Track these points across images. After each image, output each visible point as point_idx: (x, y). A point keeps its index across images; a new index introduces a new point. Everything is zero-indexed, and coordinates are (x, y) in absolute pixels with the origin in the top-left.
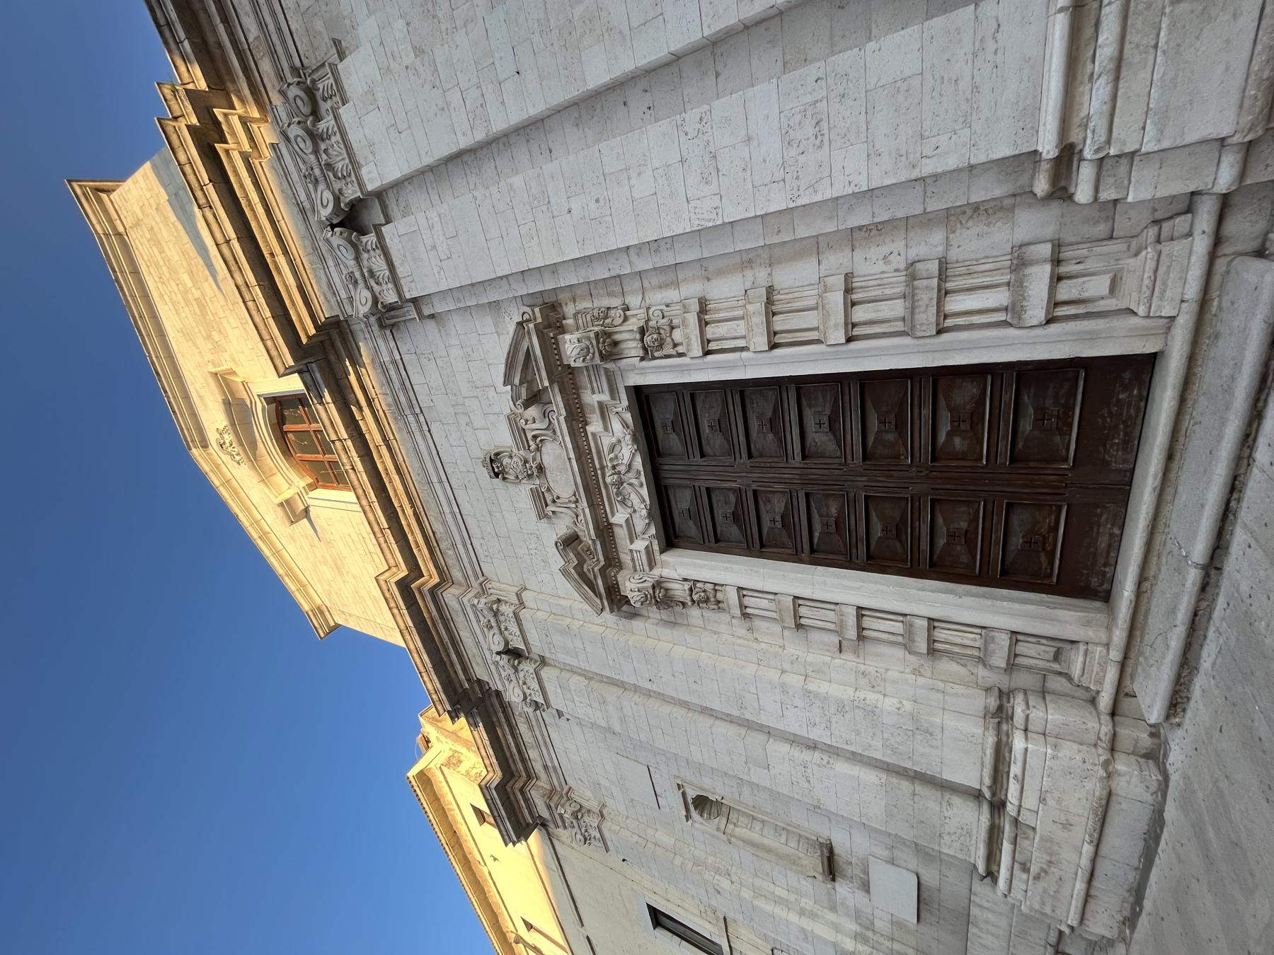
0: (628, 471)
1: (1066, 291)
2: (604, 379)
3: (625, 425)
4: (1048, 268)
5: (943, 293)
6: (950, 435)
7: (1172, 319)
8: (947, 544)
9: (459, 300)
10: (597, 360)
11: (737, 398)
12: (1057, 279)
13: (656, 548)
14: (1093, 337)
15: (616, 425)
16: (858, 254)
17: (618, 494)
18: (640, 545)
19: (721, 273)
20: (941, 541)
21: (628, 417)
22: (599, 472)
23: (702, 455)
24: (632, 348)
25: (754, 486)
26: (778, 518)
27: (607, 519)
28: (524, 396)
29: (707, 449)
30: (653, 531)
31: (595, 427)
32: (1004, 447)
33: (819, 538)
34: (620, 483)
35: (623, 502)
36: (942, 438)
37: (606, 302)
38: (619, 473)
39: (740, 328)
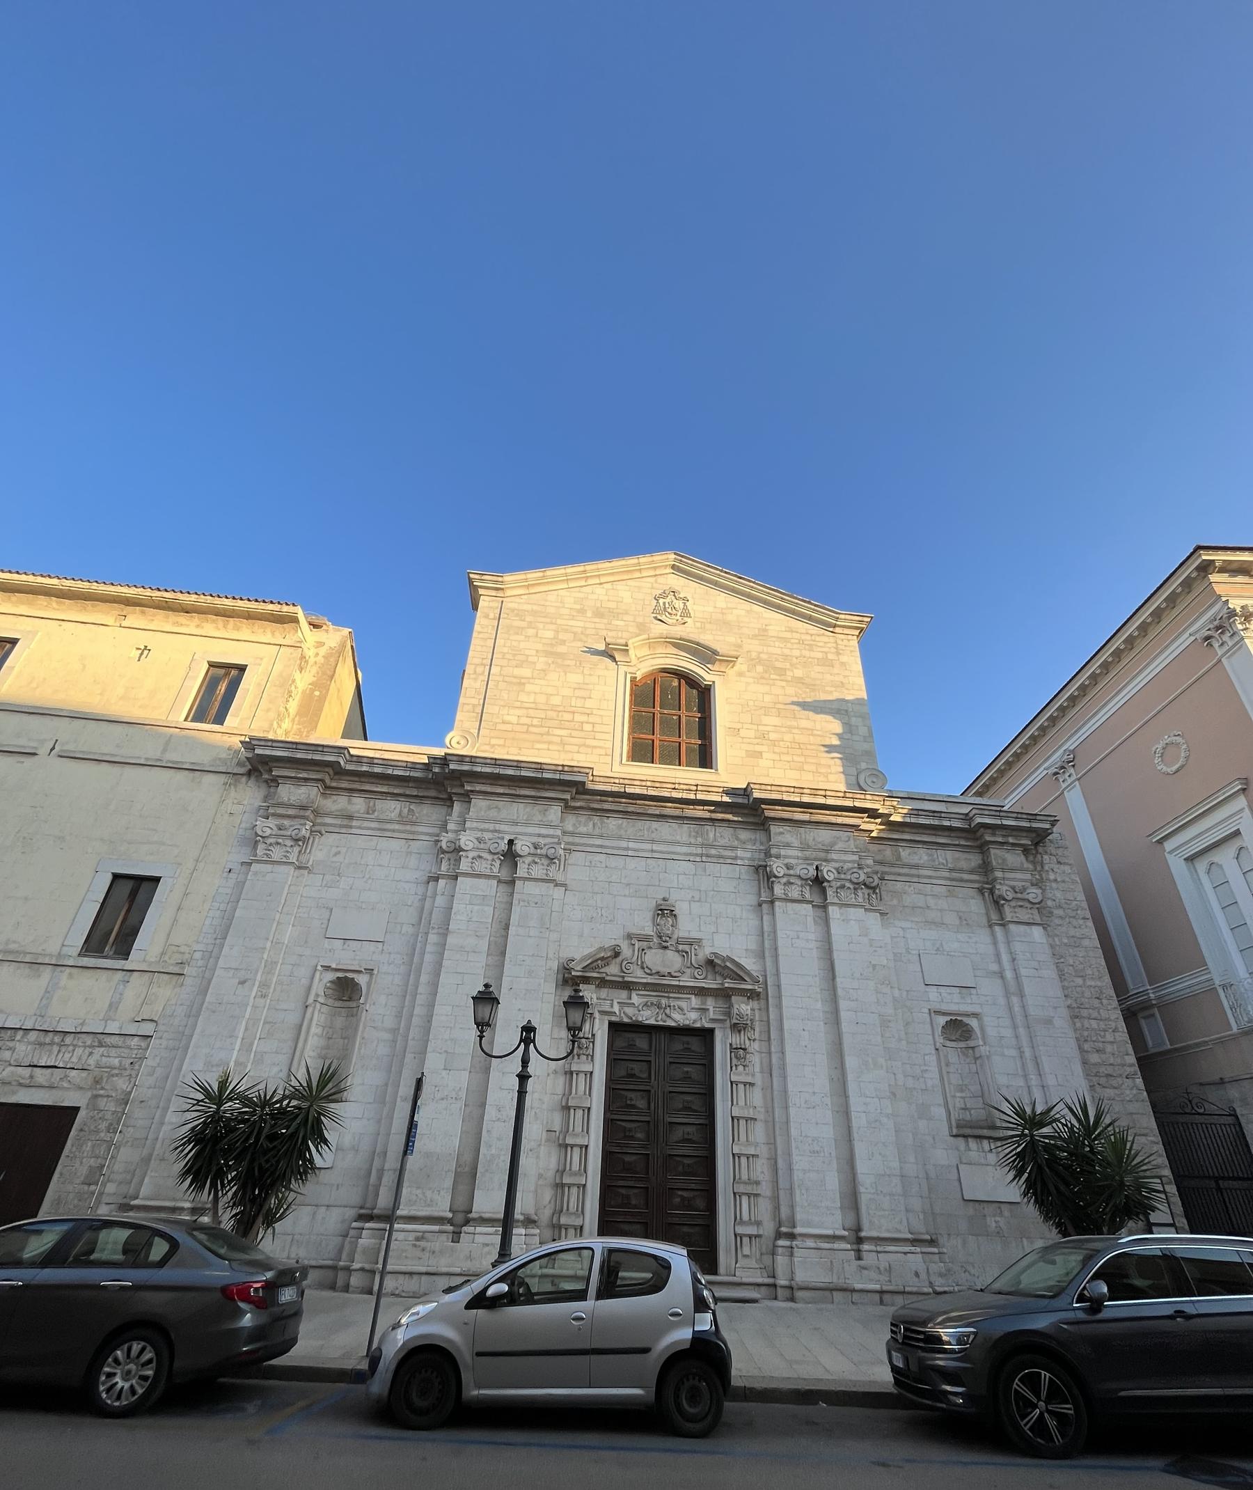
0: (666, 1014)
1: (746, 1240)
2: (721, 1018)
3: (695, 1021)
4: (756, 1233)
5: (749, 1195)
6: (681, 1196)
7: (735, 1276)
8: (623, 1195)
9: (769, 936)
10: (734, 1021)
11: (702, 1091)
12: (750, 1237)
13: (613, 1019)
14: (728, 1251)
15: (693, 1015)
16: (764, 1161)
17: (652, 1004)
18: (616, 1009)
19: (764, 1097)
20: (623, 1191)
21: (698, 1025)
22: (666, 995)
23: (670, 1063)
24: (736, 1040)
25: (653, 1091)
26: (633, 1103)
27: (636, 990)
28: (716, 960)
29: (674, 1066)
30: (626, 1020)
31: (695, 1001)
32: (676, 1220)
33: (621, 1125)
34: (659, 1006)
35: (646, 1005)
36: (680, 1193)
37: (757, 1029)
38: (665, 1008)
39: (742, 1103)
